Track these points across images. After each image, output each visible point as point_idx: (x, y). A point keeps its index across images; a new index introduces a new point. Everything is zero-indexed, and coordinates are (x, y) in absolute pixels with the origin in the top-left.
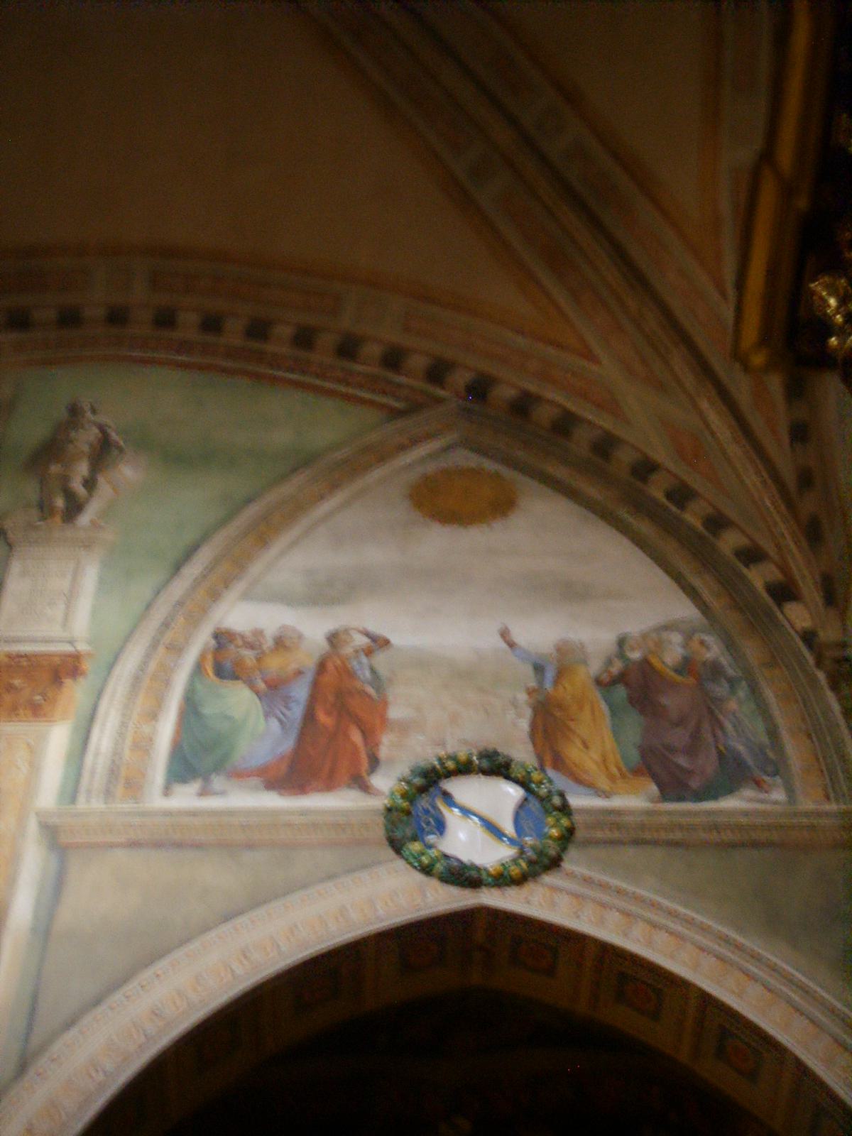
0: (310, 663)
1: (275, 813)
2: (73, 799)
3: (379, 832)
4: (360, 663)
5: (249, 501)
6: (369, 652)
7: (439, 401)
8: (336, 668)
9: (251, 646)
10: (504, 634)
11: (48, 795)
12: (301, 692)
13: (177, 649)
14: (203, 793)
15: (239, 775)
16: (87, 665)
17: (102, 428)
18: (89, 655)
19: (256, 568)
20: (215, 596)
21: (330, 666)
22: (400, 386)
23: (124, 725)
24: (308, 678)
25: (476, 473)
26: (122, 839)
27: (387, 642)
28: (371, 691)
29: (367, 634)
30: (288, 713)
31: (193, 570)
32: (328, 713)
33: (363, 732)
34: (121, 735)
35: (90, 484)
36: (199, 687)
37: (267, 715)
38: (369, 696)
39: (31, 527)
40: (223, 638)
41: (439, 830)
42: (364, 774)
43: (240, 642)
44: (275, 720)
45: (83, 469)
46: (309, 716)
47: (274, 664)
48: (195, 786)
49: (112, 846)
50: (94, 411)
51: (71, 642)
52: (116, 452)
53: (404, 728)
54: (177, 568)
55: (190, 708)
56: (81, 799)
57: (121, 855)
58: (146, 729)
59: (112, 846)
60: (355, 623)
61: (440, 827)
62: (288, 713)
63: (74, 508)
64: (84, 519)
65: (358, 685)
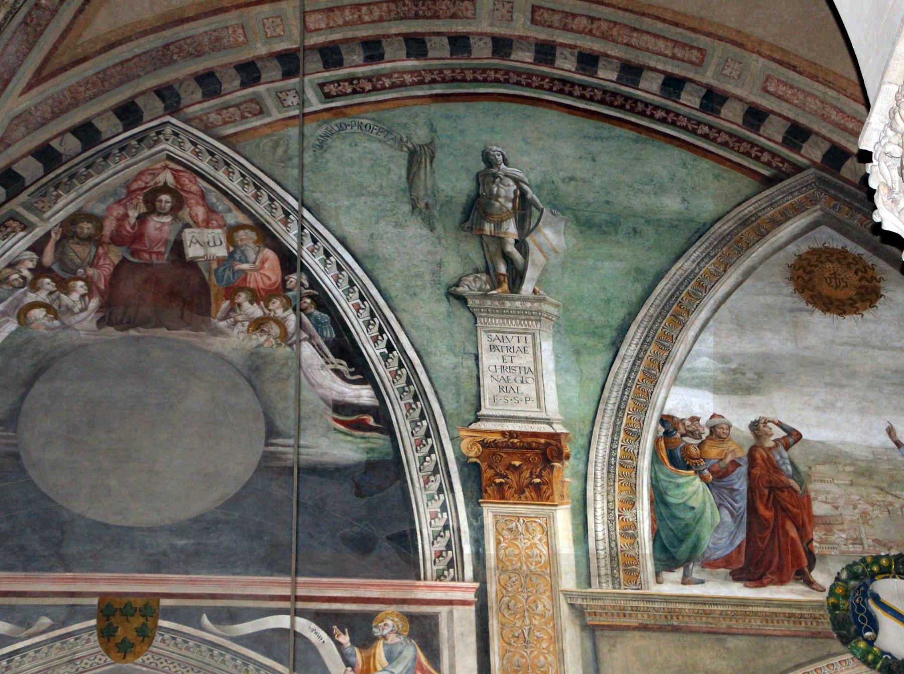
0: (742, 454)
1: (743, 602)
2: (590, 585)
3: (826, 625)
4: (781, 457)
5: (659, 277)
6: (787, 447)
7: (798, 169)
8: (763, 460)
9: (692, 434)
10: (890, 431)
11: (568, 581)
12: (740, 482)
13: (636, 436)
14: (685, 581)
15: (711, 564)
16: (568, 448)
17: (517, 181)
18: (567, 434)
19: (680, 350)
20: (653, 380)
21: (758, 456)
22: (763, 150)
23: (610, 511)
24: (743, 469)
25: (842, 255)
26: (633, 622)
27: (799, 436)
28: (796, 486)
29: (780, 425)
30: (735, 504)
31: (629, 349)
32: (767, 507)
33: (798, 530)
34: (611, 521)
35: (521, 245)
36: (662, 476)
37: (719, 506)
38: (796, 491)
39: (485, 296)
40: (665, 420)
41: (872, 627)
42: (806, 570)
43: (682, 430)
44: (727, 512)
45: (511, 229)
46: (751, 508)
47: (713, 452)
48: (678, 574)
49: (629, 628)
50: (506, 164)
51: (549, 422)
52: (536, 213)
53: (828, 523)
54: (616, 346)
55: (659, 499)
56: (594, 580)
57: (637, 640)
58: (628, 515)
59: (629, 628)
60: (770, 416)
61: (874, 625)
62: (735, 504)
63: (516, 277)
64: (527, 288)
65: (783, 478)
